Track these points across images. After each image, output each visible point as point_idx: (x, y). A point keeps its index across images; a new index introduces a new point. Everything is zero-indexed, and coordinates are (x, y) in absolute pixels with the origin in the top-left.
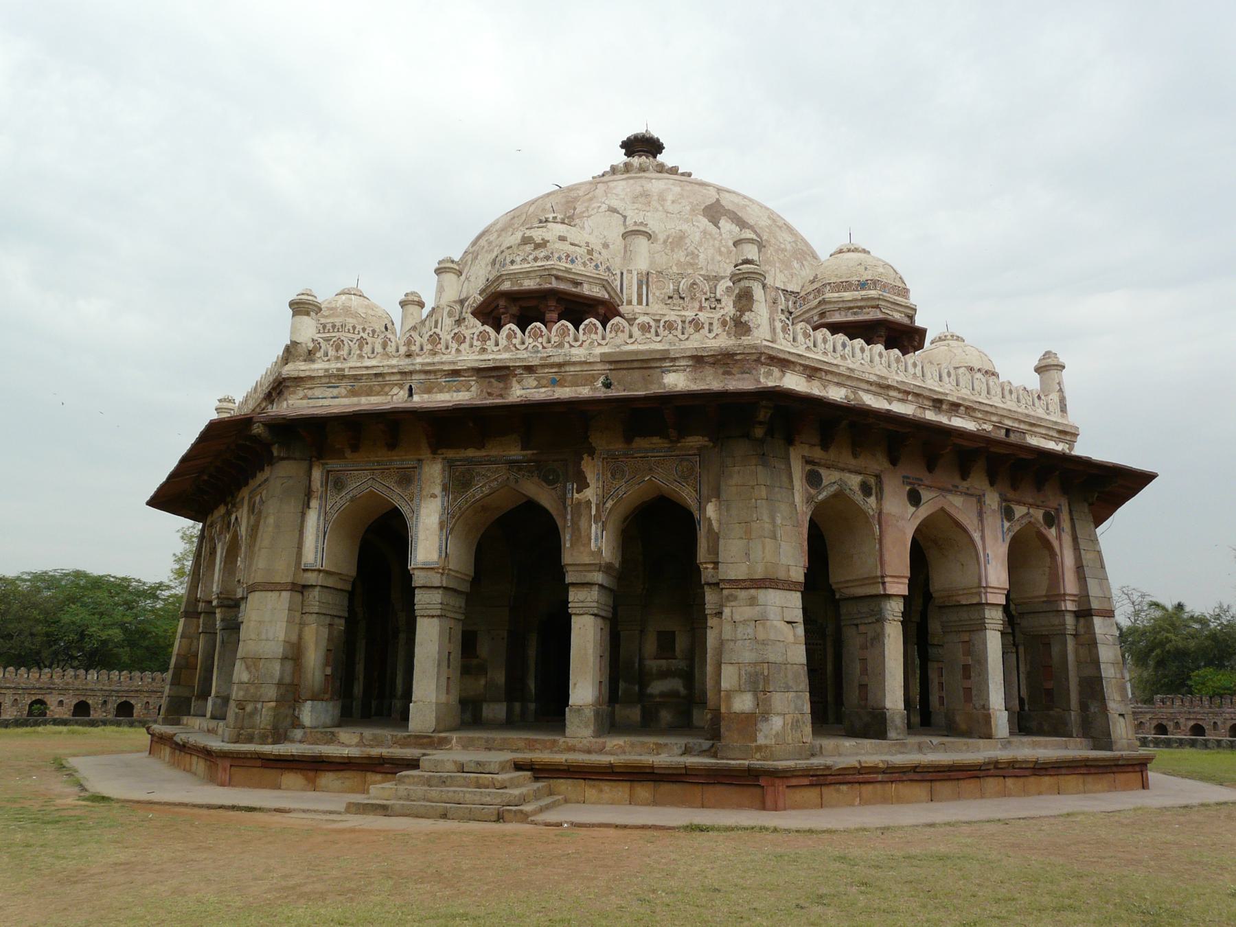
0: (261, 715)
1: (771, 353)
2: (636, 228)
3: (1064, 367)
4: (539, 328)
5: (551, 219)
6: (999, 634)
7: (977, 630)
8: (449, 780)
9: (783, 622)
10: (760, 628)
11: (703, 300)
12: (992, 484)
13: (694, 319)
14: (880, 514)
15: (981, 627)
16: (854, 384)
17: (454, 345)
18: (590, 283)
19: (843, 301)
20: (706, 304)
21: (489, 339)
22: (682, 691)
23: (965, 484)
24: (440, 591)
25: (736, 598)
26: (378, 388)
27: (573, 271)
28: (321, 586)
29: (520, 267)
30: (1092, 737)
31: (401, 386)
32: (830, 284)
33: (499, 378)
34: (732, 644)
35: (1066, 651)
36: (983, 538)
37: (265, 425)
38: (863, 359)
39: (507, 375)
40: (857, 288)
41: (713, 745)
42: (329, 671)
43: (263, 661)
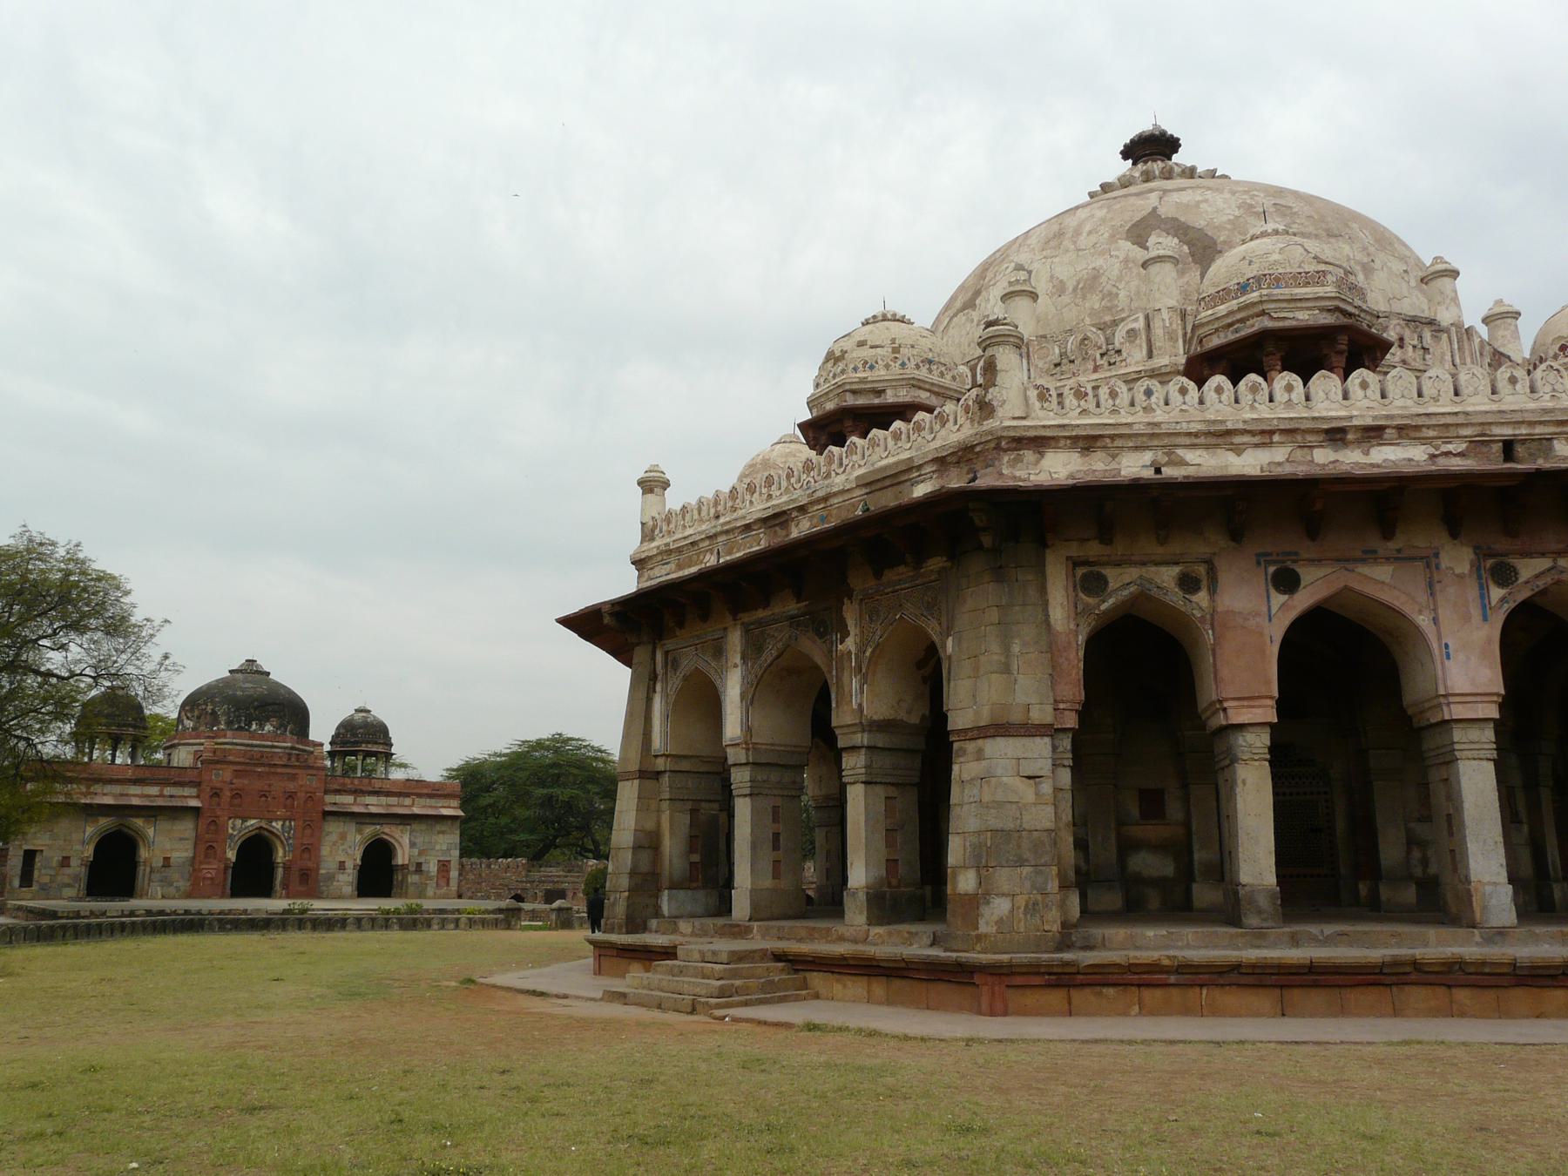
1: (1013, 434)
2: (1012, 289)
9: (1017, 778)
11: (1098, 356)
16: (1166, 441)
18: (895, 387)
19: (1218, 319)
20: (1104, 362)
24: (749, 768)
27: (869, 379)
28: (671, 771)
31: (711, 551)
33: (781, 524)
36: (1435, 621)
38: (1184, 403)
39: (786, 521)
40: (1236, 294)
42: (696, 858)
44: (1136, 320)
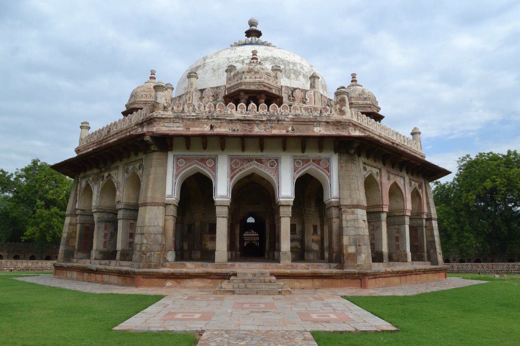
0: (154, 257)
3: (421, 133)
4: (265, 106)
5: (255, 62)
6: (408, 226)
7: (402, 224)
8: (253, 280)
10: (356, 223)
12: (407, 173)
13: (324, 108)
14: (381, 183)
15: (404, 223)
17: (230, 110)
21: (244, 108)
22: (299, 247)
23: (401, 174)
25: (347, 212)
26: (197, 124)
27: (270, 84)
28: (174, 205)
29: (249, 80)
30: (430, 261)
32: (353, 97)
33: (249, 124)
34: (347, 228)
35: (423, 232)
37: (151, 137)
41: (338, 265)
43: (153, 235)
44: (312, 92)
